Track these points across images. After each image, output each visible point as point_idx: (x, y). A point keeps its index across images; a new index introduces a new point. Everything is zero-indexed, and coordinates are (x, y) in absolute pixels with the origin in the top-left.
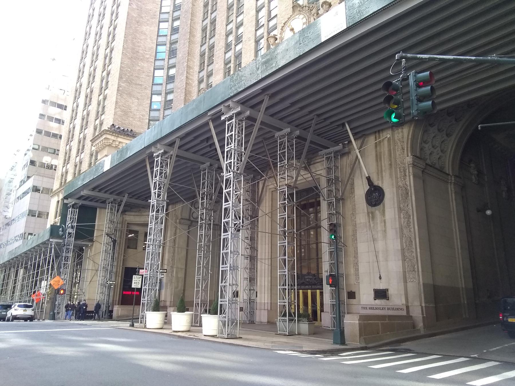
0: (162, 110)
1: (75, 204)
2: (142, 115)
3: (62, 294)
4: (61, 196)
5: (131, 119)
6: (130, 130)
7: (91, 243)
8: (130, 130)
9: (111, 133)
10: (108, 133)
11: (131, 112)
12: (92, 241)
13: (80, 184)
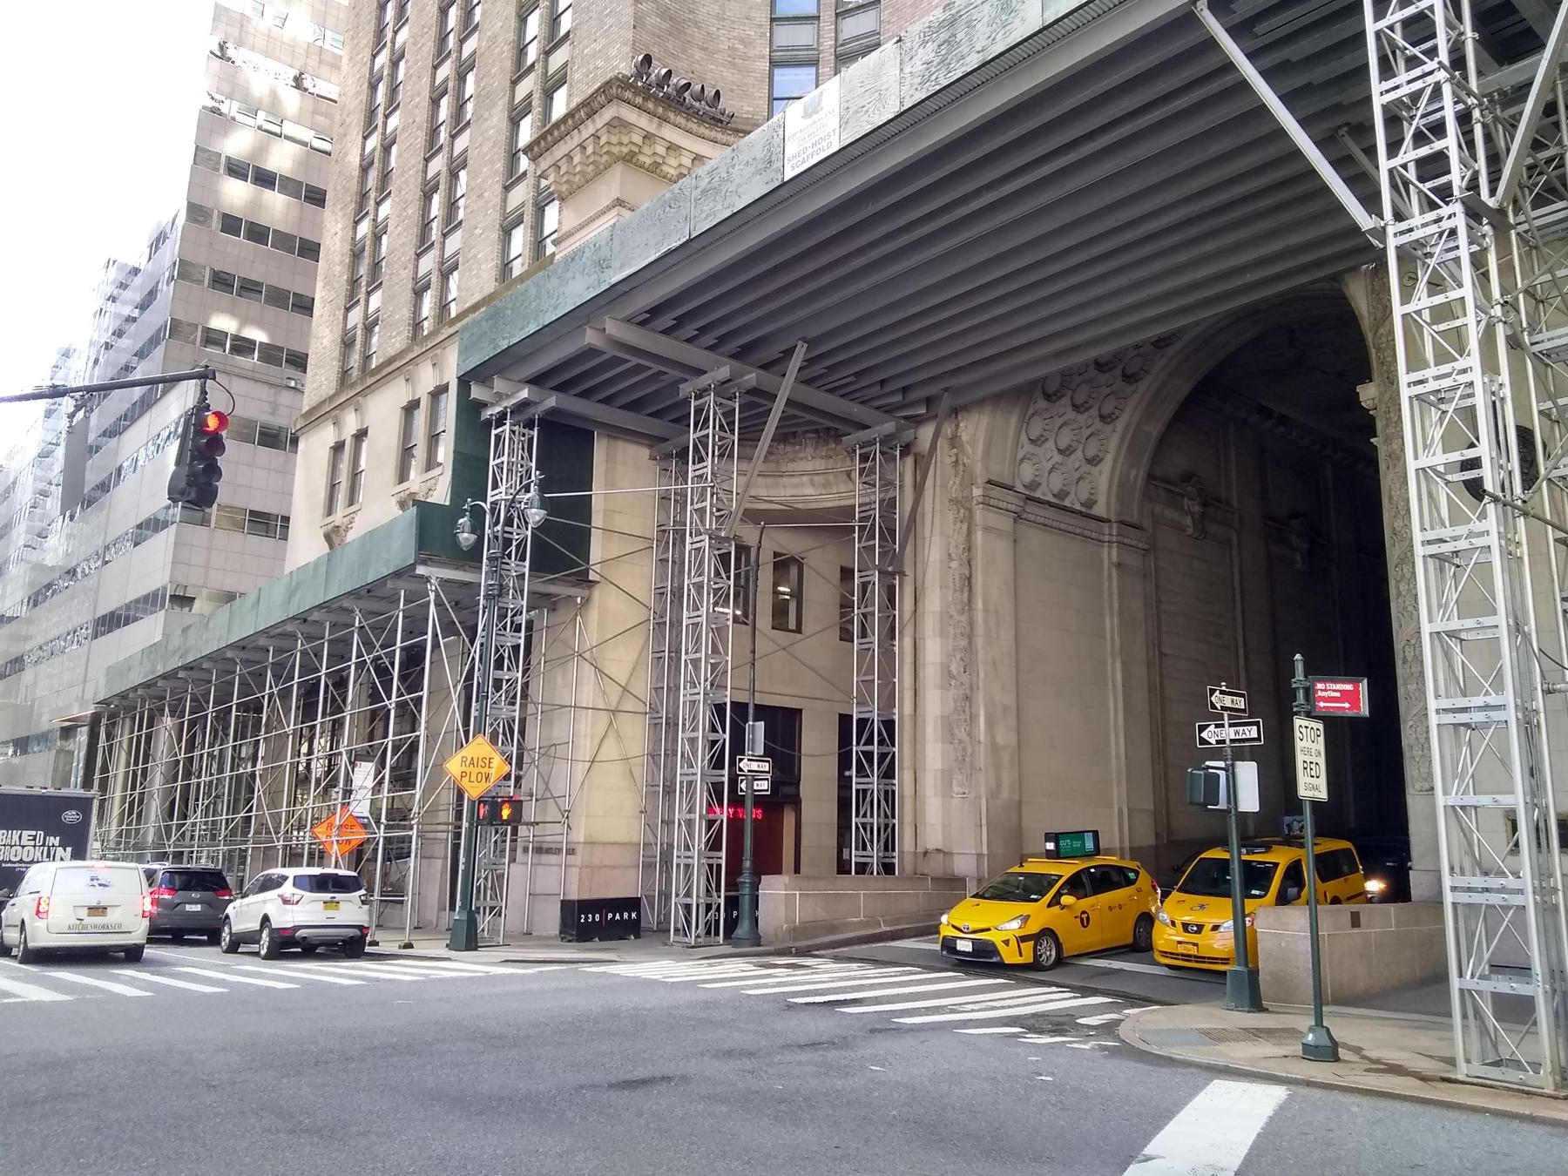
0: (828, 16)
1: (524, 404)
2: (742, 41)
3: (507, 822)
4: (452, 367)
5: (698, 55)
6: (710, 92)
7: (586, 593)
8: (710, 92)
9: (639, 100)
10: (628, 95)
11: (696, 24)
12: (583, 580)
13: (578, 290)
